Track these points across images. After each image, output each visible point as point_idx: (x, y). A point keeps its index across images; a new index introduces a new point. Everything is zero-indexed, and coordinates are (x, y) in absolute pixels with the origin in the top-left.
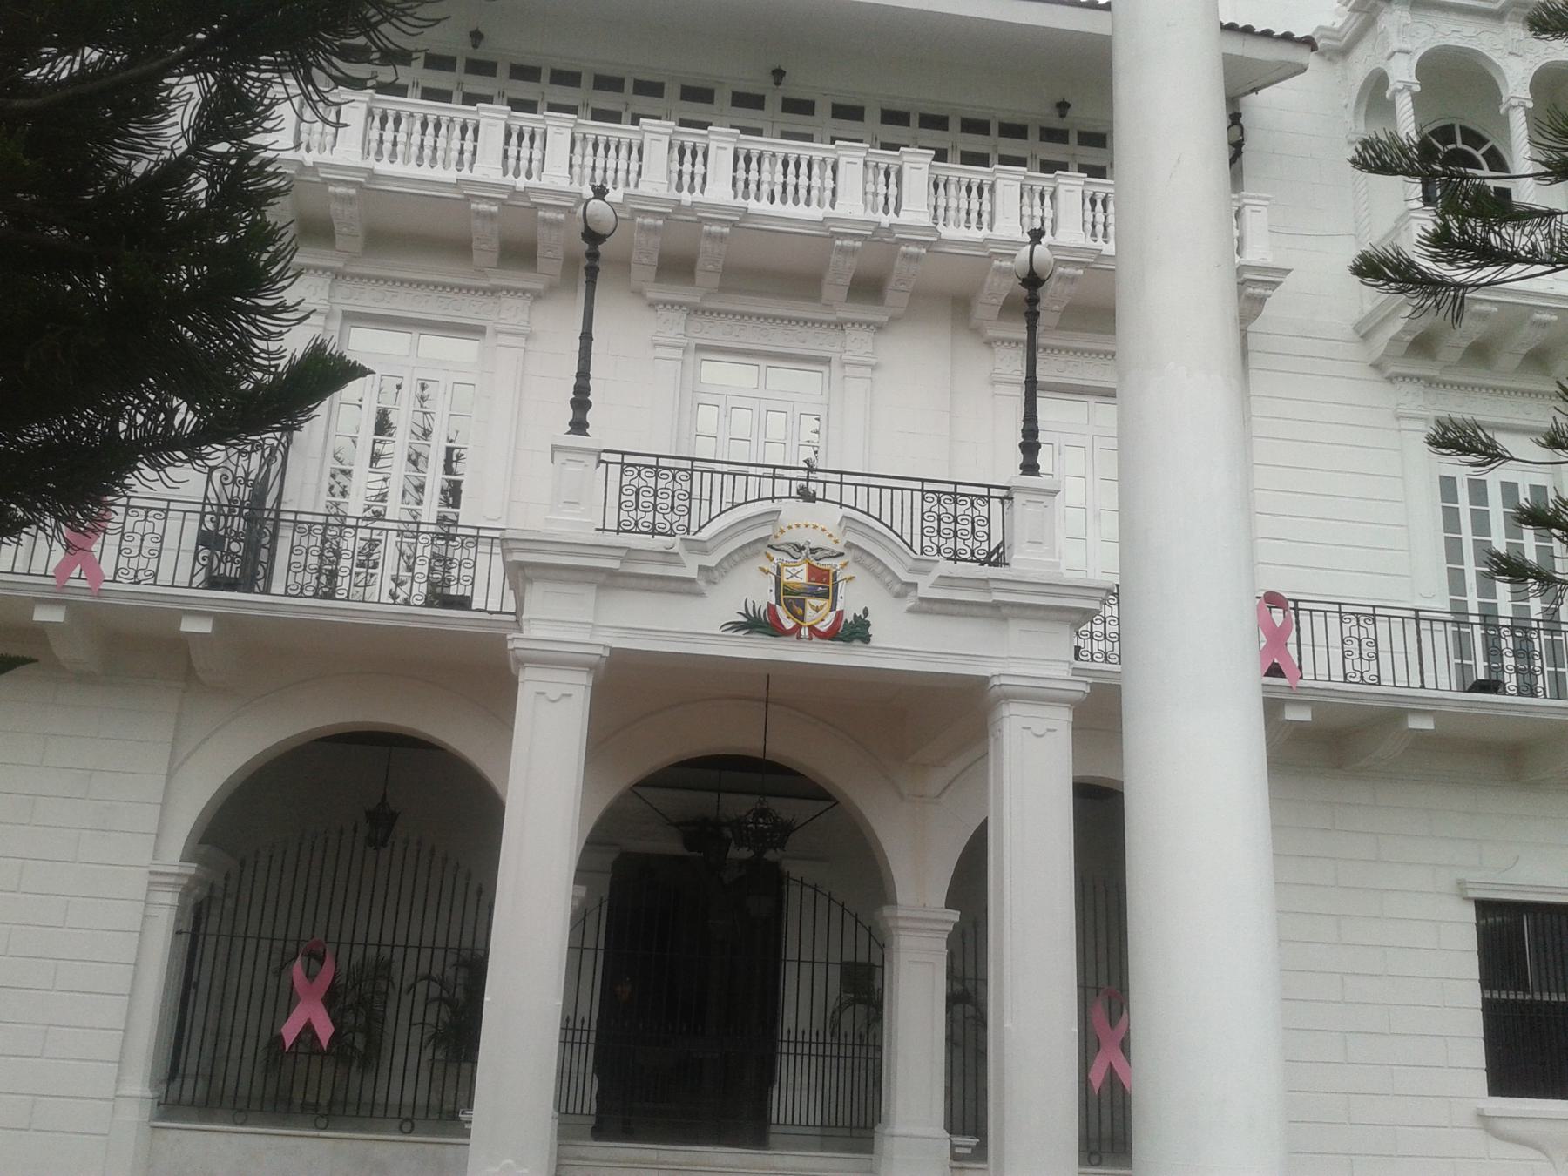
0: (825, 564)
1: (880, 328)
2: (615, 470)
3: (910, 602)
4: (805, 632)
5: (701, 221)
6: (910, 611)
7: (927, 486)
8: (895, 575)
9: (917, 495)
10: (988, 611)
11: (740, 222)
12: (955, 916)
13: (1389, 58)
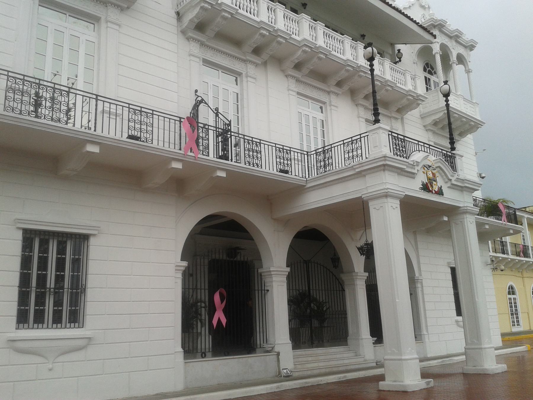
6: (448, 187)
10: (460, 188)
12: (367, 274)
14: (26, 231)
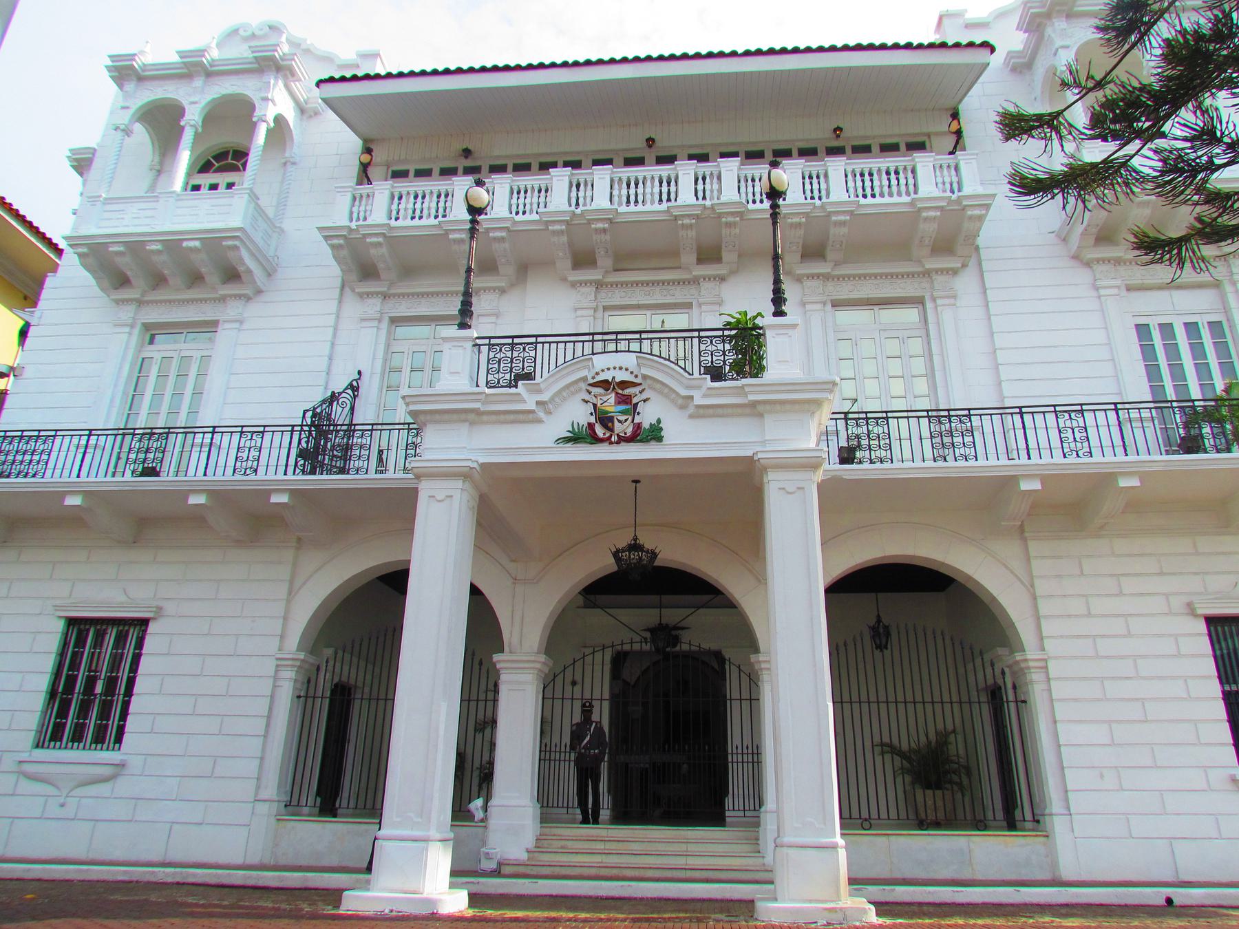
0: (627, 392)
1: (722, 279)
2: (485, 349)
3: (691, 410)
4: (614, 438)
5: (590, 222)
6: (691, 417)
7: (702, 334)
8: (677, 394)
9: (696, 341)
10: (748, 411)
11: (612, 221)
13: (1055, 54)
14: (72, 622)
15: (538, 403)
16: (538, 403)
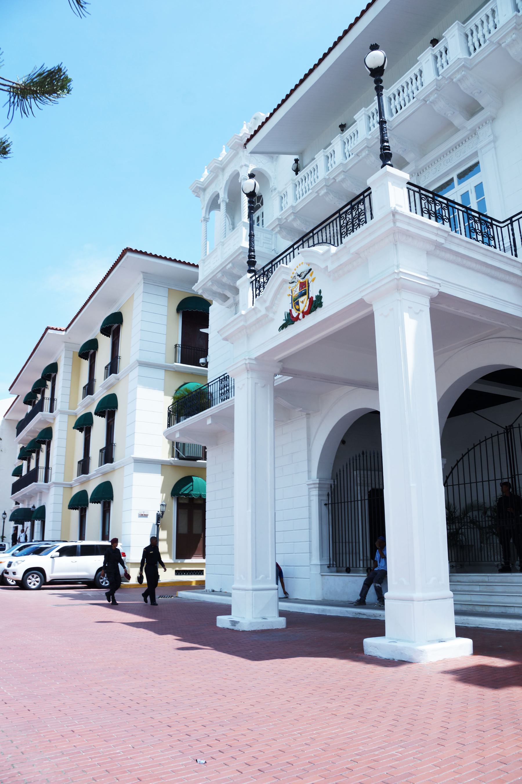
1: (493, 119)
4: (301, 316)
15: (267, 309)
16: (267, 309)
